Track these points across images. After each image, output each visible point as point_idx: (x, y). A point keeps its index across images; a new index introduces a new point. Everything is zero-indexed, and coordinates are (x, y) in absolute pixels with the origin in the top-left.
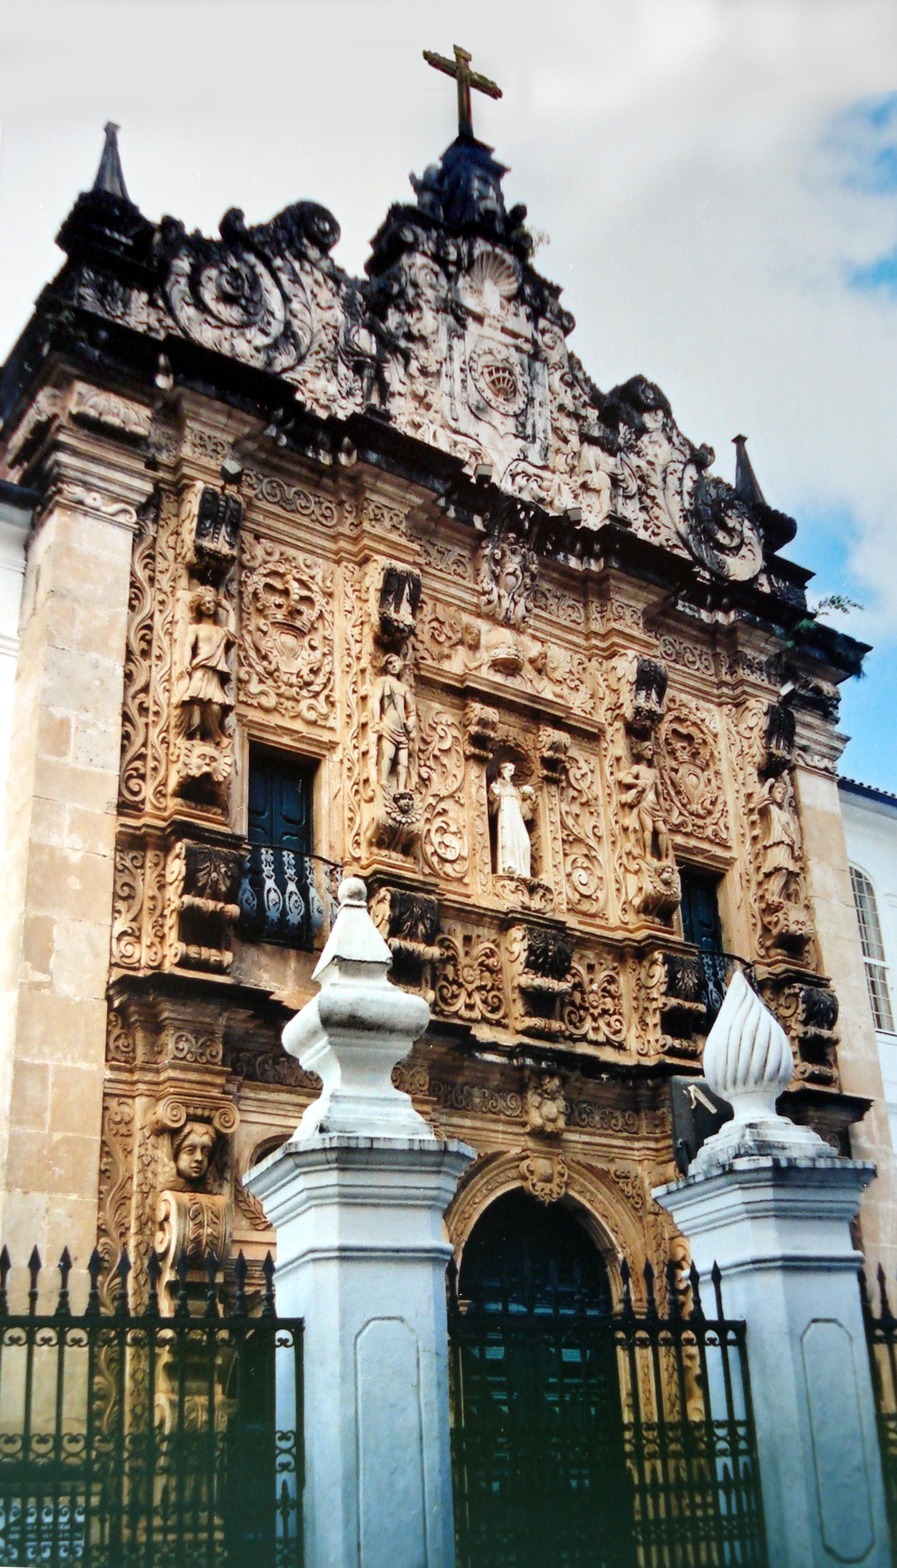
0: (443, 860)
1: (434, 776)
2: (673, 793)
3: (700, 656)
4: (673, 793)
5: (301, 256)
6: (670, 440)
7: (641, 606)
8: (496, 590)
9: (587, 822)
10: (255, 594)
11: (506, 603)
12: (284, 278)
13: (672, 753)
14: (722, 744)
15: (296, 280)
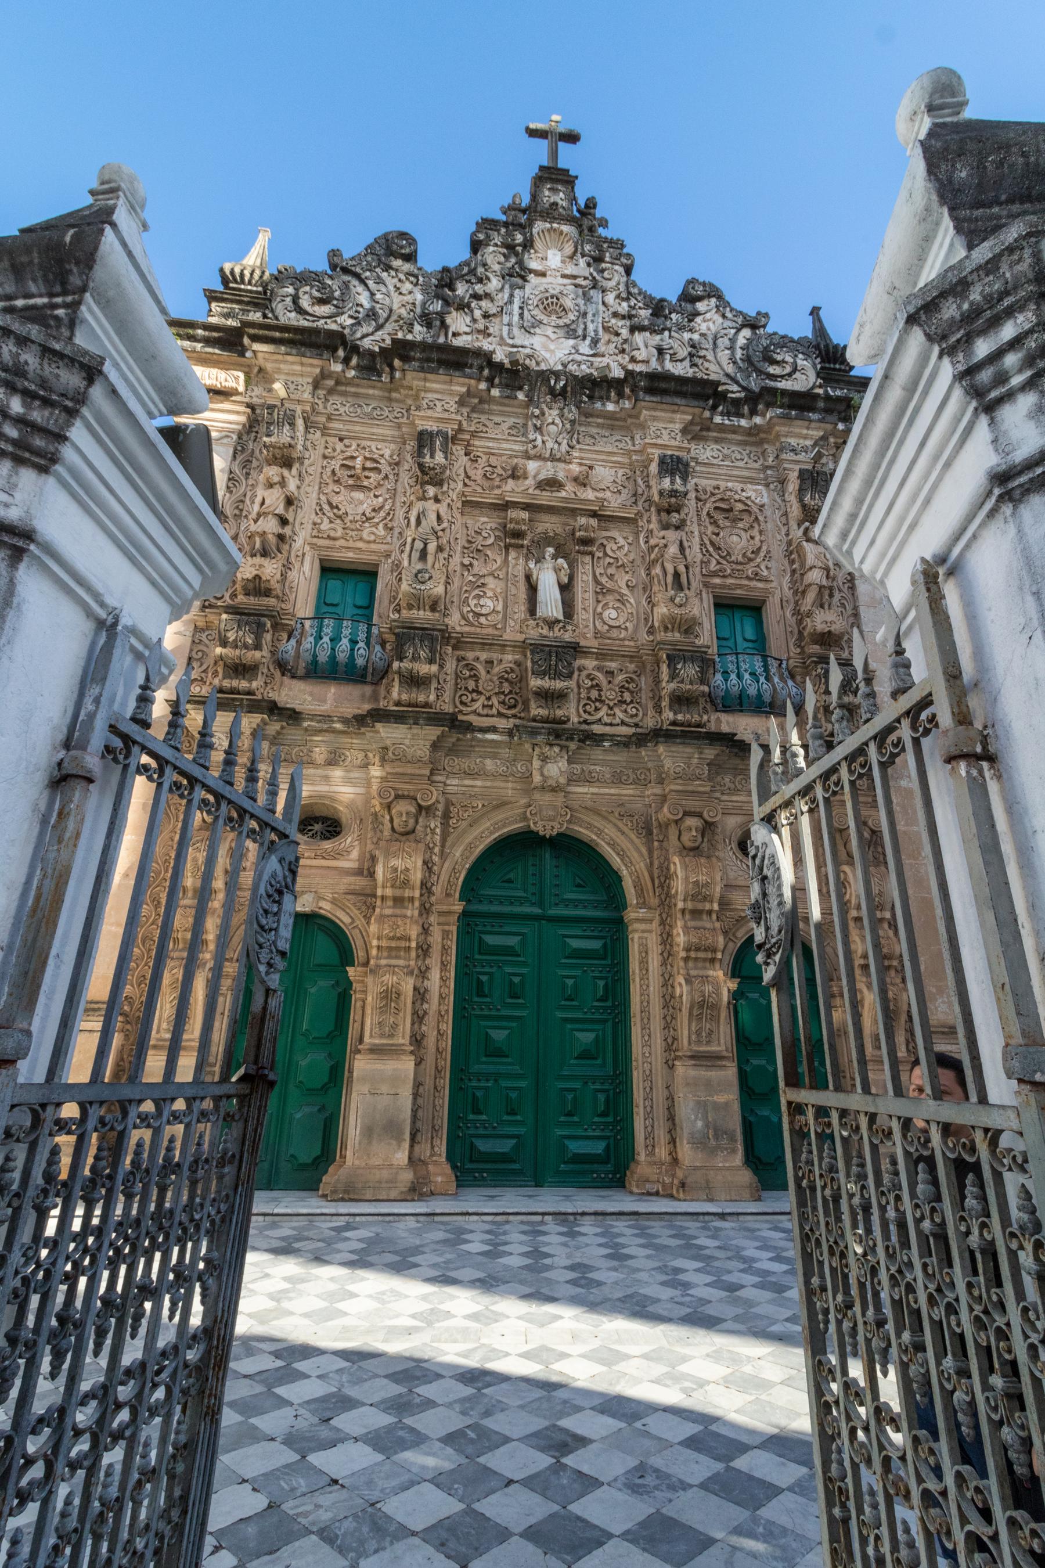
0: (478, 615)
1: (475, 563)
2: (711, 549)
3: (749, 455)
4: (711, 549)
5: (388, 268)
6: (724, 316)
7: (678, 426)
8: (539, 438)
9: (622, 579)
10: (333, 472)
11: (550, 444)
12: (370, 283)
13: (715, 523)
14: (768, 512)
15: (380, 281)
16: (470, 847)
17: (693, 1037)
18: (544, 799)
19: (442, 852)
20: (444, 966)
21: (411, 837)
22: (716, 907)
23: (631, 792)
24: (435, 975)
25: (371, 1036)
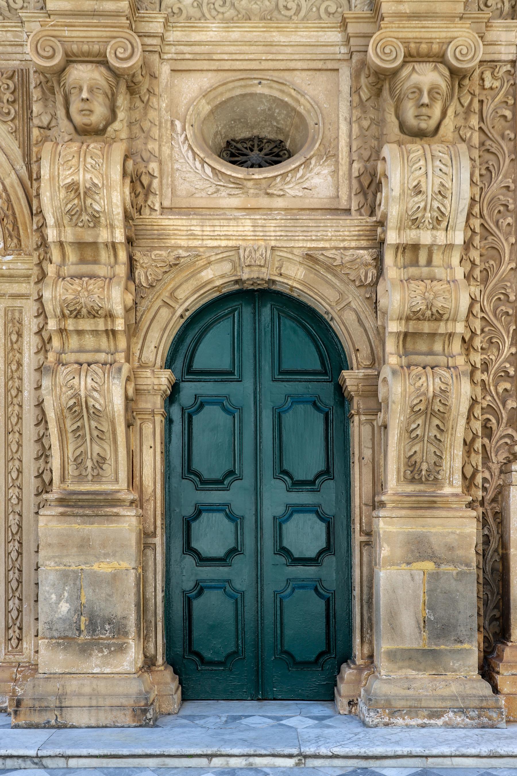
17: (71, 469)
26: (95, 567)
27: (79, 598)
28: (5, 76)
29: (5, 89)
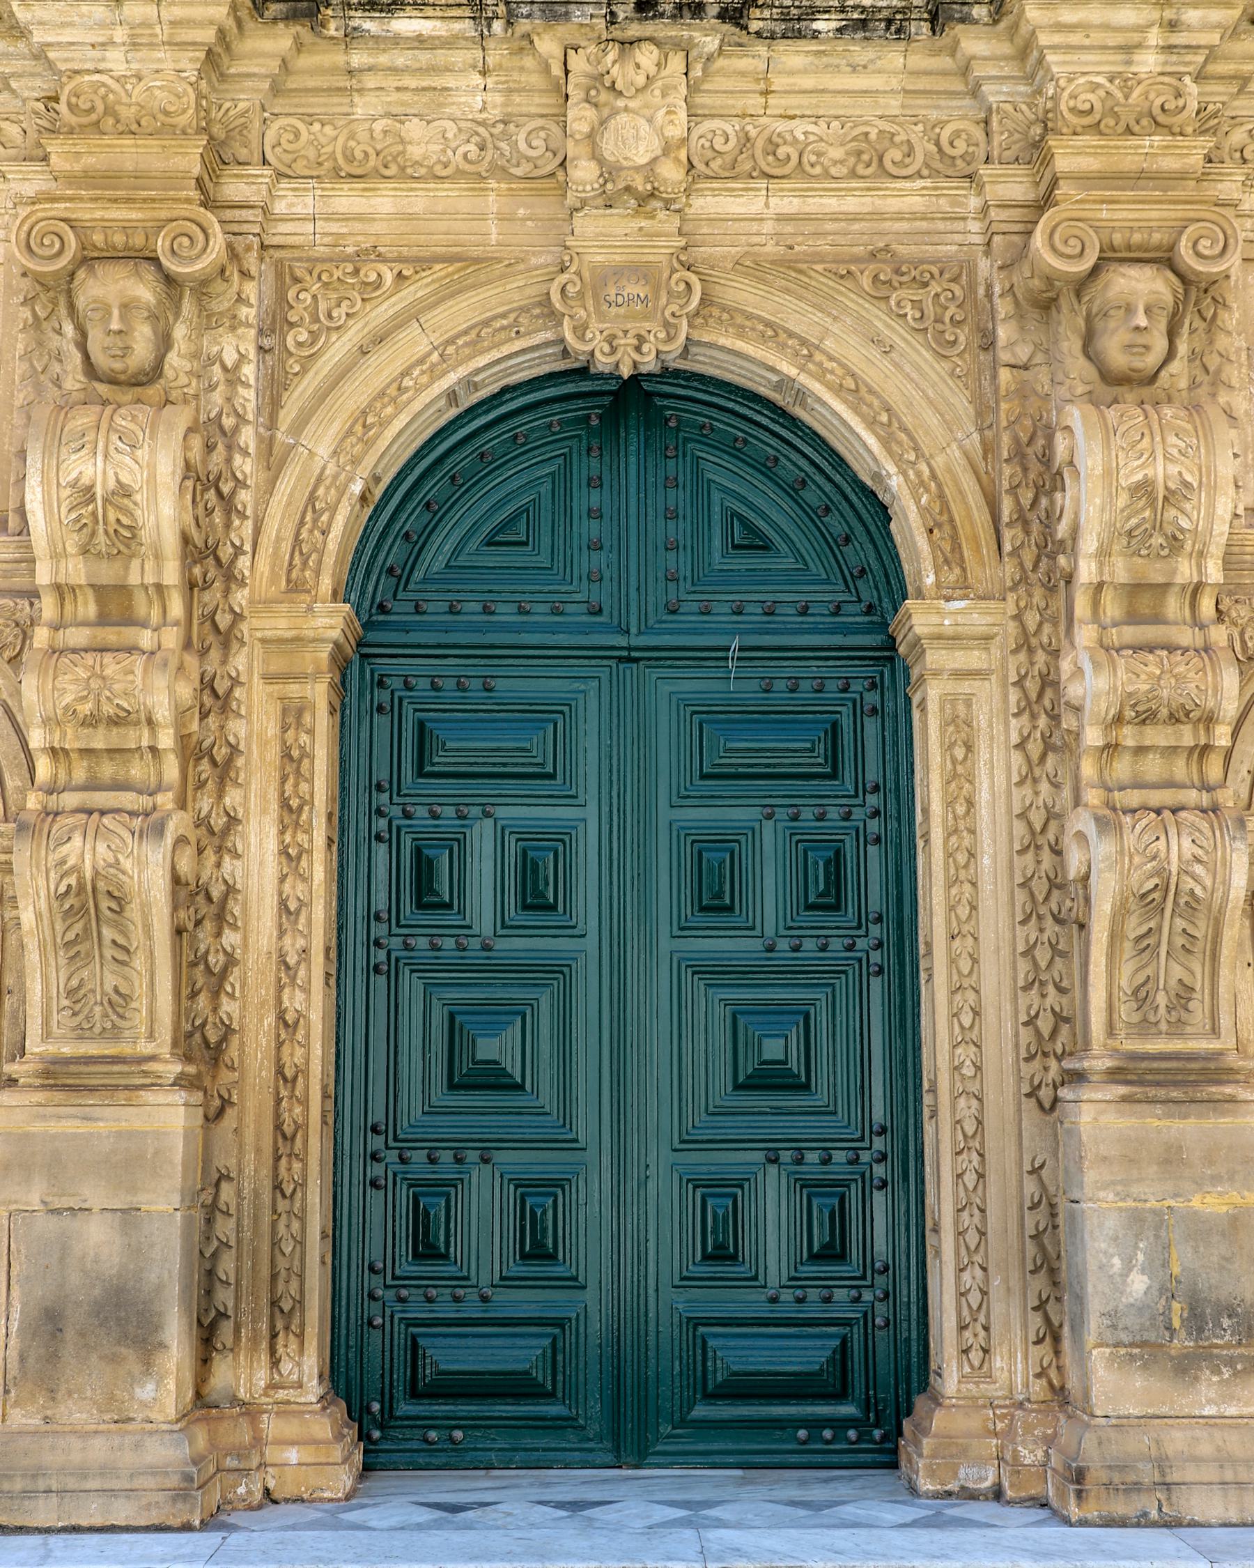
16: (364, 424)
17: (1125, 1011)
18: (605, 237)
19: (267, 444)
20: (291, 813)
21: (153, 391)
22: (1214, 573)
23: (916, 203)
24: (260, 841)
25: (47, 1035)
26: (1196, 1203)
27: (1166, 1264)
28: (947, 276)
29: (947, 299)
